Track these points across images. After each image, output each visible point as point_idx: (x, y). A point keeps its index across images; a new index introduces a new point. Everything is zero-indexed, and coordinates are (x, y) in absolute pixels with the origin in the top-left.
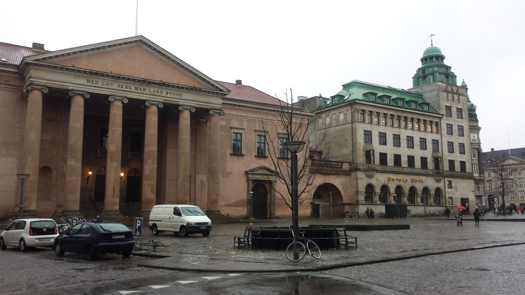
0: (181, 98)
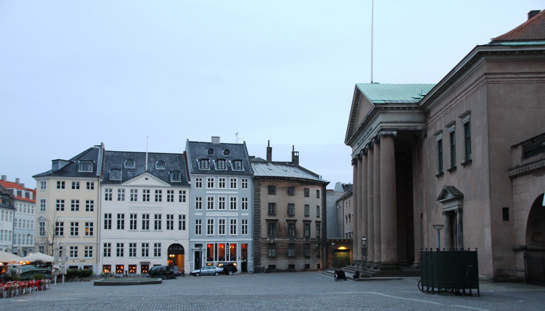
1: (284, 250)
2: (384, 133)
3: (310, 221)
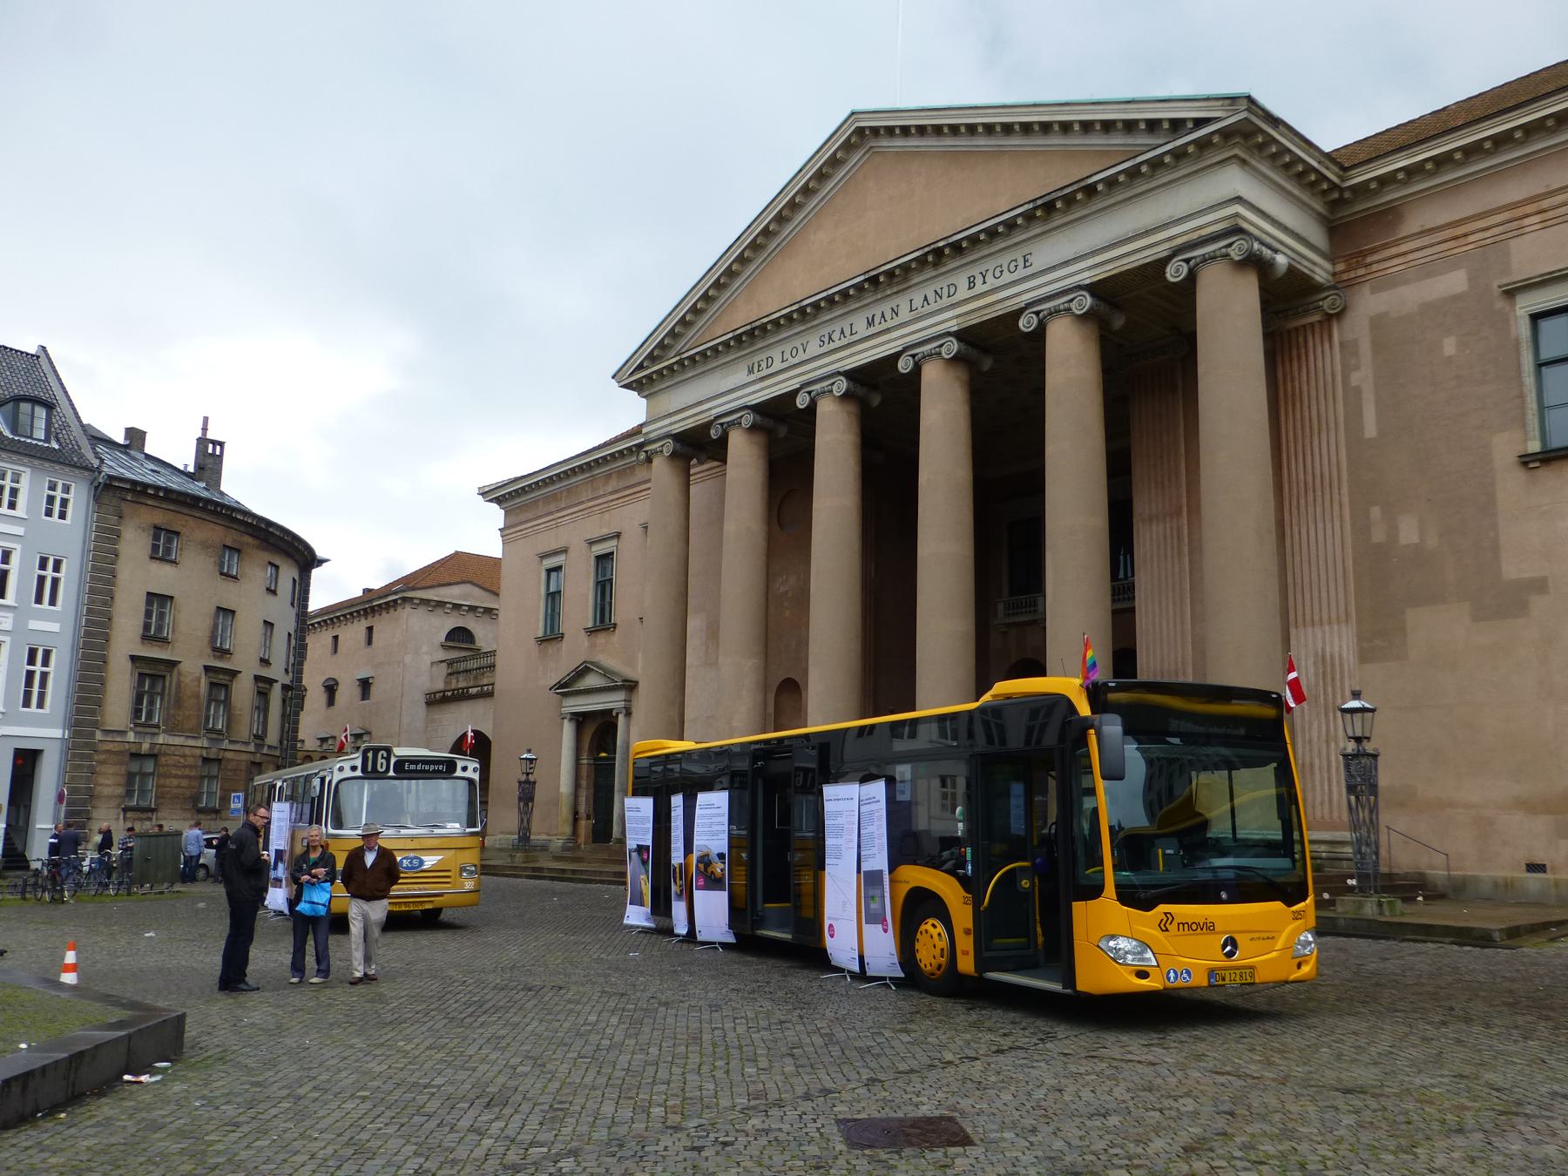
0: (1029, 271)
1: (185, 783)
3: (271, 682)
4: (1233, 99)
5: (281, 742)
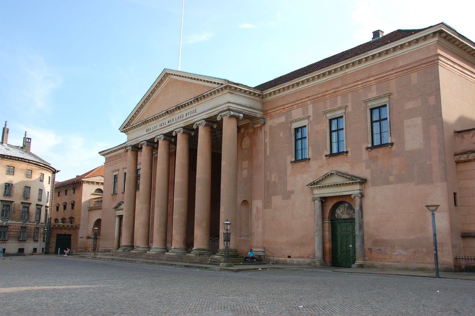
0: (196, 114)
1: (16, 233)
2: (232, 113)
3: (41, 206)
4: (226, 80)
5: (46, 221)
